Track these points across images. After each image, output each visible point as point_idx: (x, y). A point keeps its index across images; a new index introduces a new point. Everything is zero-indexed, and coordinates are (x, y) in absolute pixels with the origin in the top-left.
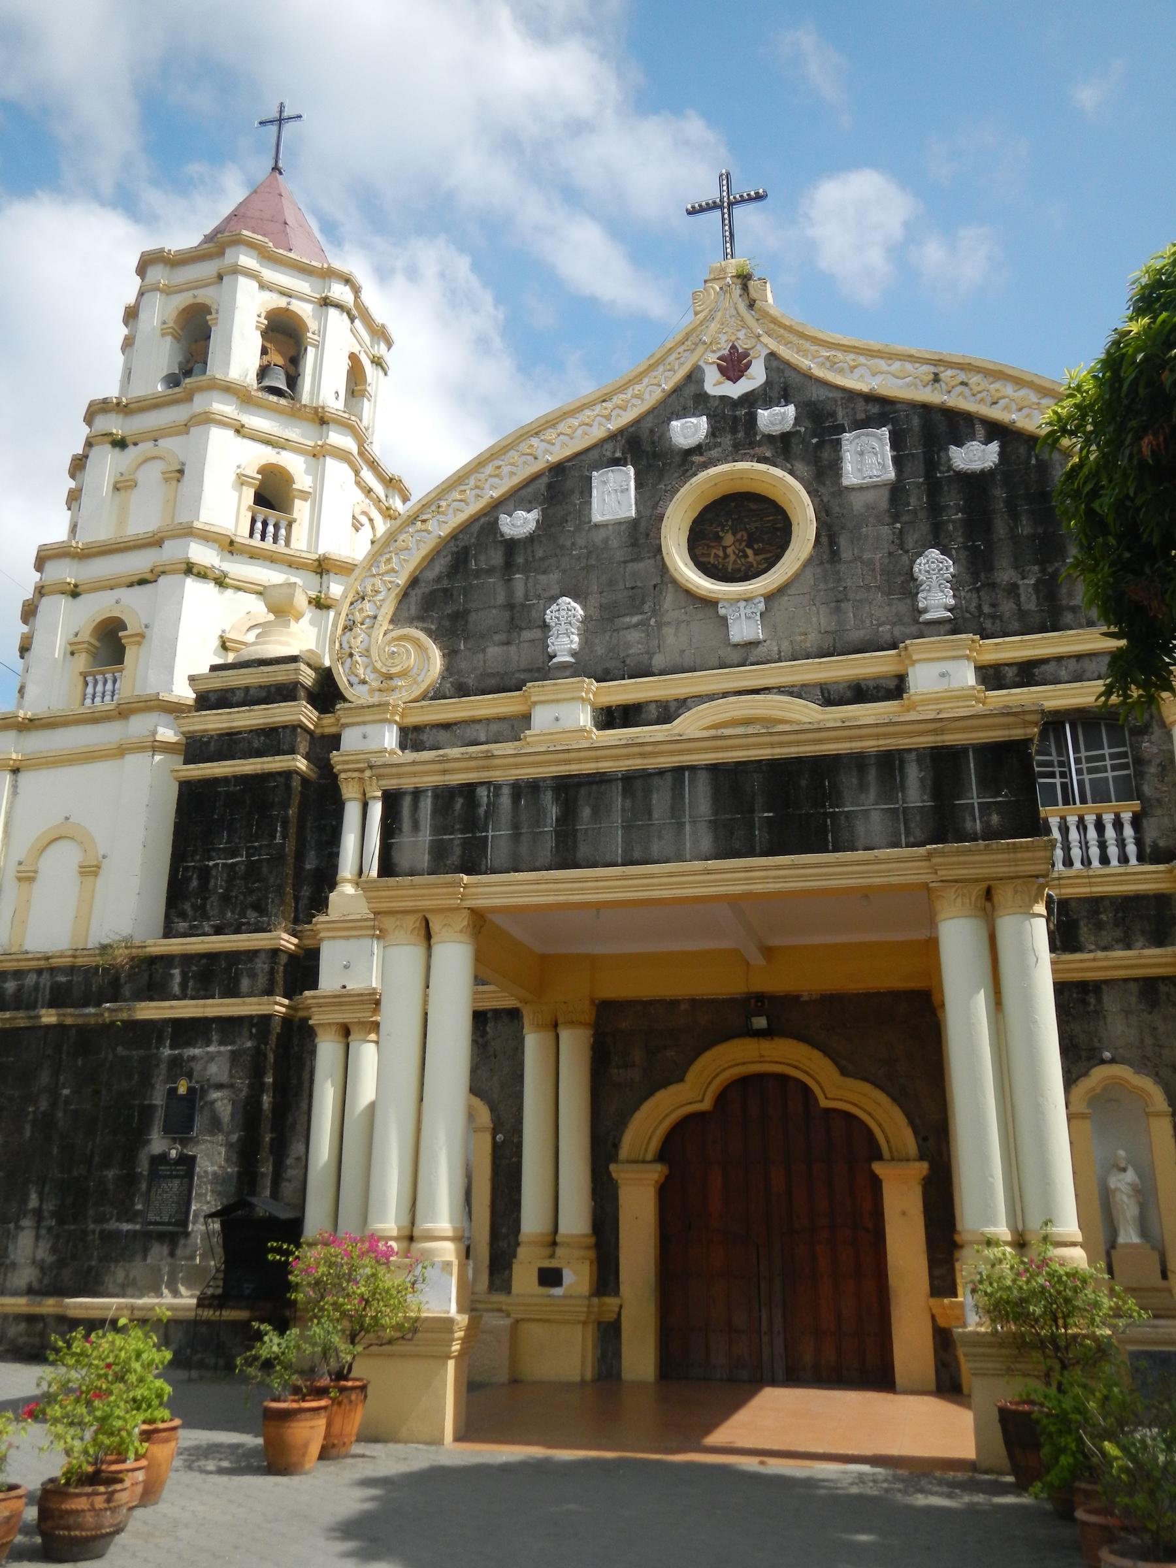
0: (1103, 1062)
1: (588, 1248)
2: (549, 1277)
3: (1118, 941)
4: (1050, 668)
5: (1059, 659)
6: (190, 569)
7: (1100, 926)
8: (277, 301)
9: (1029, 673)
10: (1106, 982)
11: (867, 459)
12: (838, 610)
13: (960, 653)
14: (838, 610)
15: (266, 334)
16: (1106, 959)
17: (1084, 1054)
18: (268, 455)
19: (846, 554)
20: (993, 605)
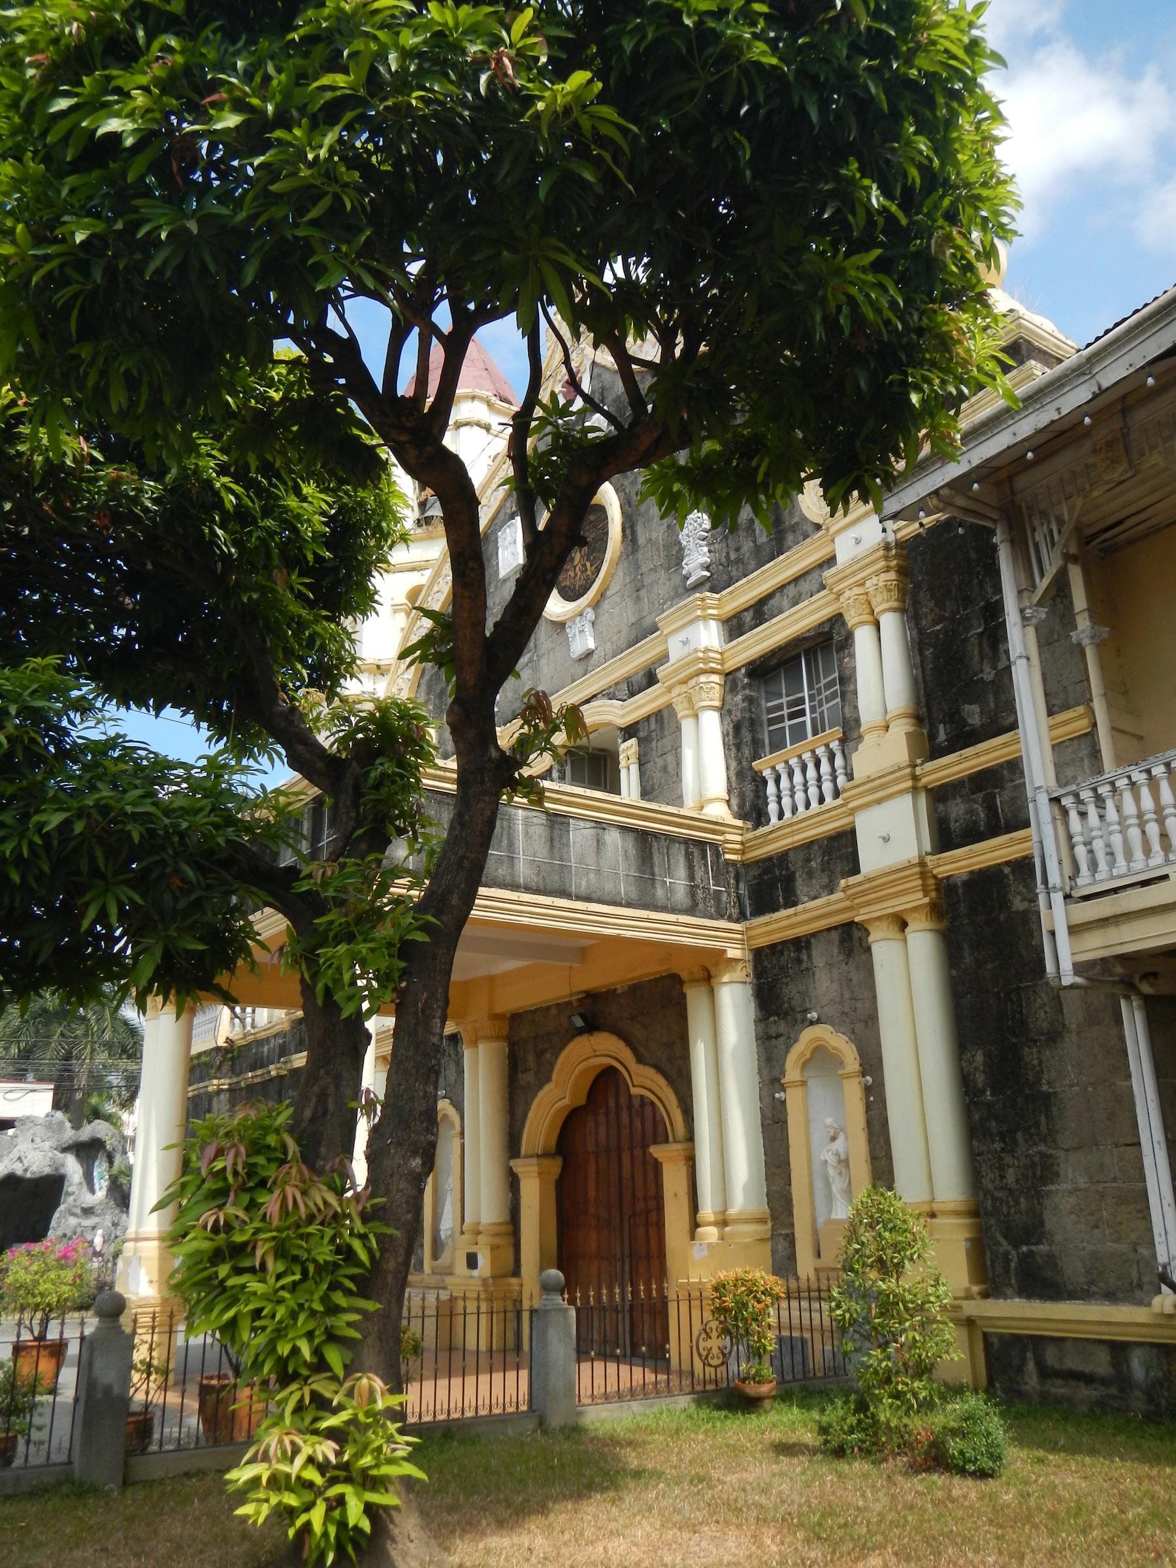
0: (812, 1023)
1: (497, 1235)
2: (472, 1261)
3: (824, 887)
4: (773, 602)
5: (782, 588)
7: (810, 874)
9: (760, 611)
10: (814, 935)
12: (638, 599)
13: (693, 616)
14: (638, 599)
16: (829, 904)
17: (799, 1016)
19: (641, 541)
20: (737, 550)
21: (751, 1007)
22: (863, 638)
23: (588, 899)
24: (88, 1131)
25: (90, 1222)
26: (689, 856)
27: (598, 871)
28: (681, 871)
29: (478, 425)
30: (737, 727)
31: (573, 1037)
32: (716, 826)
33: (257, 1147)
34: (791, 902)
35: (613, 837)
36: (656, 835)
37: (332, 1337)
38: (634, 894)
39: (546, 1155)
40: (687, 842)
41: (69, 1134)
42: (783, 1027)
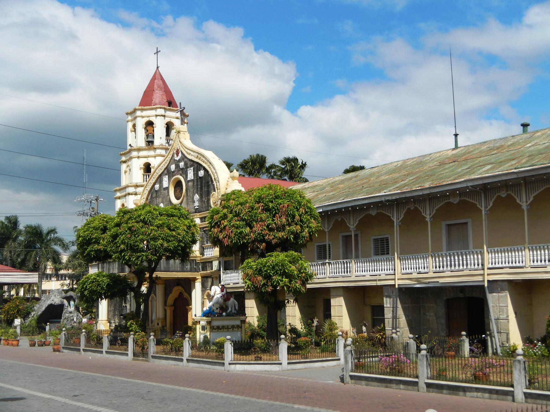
2: (158, 324)
6: (129, 194)
8: (146, 119)
11: (191, 175)
15: (145, 128)
18: (145, 160)
25: (71, 315)
28: (189, 265)
29: (162, 116)
39: (171, 306)
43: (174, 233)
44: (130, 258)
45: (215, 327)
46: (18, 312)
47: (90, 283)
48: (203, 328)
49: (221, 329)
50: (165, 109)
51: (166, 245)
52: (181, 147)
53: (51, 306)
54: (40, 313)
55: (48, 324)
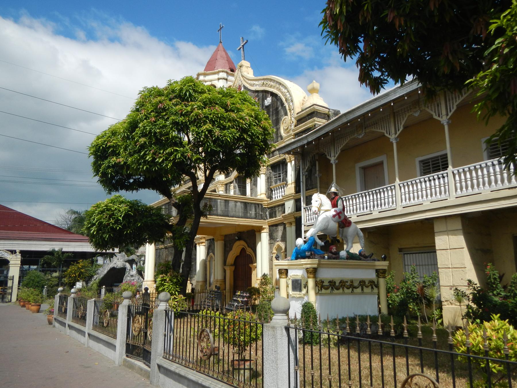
21: (268, 236)
22: (289, 164)
23: (233, 217)
24: (131, 257)
25: (132, 278)
26: (255, 207)
27: (235, 211)
28: (254, 210)
29: (224, 79)
30: (268, 178)
31: (235, 242)
32: (262, 200)
33: (167, 267)
34: (276, 217)
35: (239, 204)
36: (248, 203)
37: (177, 291)
38: (243, 215)
39: (231, 265)
40: (255, 204)
41: (126, 258)
42: (273, 242)
43: (233, 115)
44: (154, 159)
45: (326, 283)
46: (79, 275)
47: (99, 214)
48: (297, 285)
49: (338, 289)
50: (227, 73)
51: (217, 132)
52: (243, 82)
53: (113, 269)
54: (102, 276)
55: (104, 286)
